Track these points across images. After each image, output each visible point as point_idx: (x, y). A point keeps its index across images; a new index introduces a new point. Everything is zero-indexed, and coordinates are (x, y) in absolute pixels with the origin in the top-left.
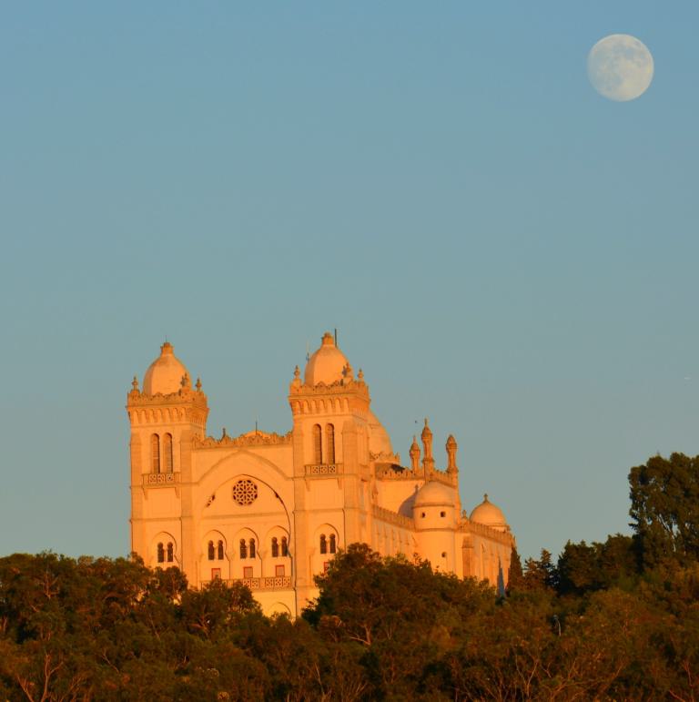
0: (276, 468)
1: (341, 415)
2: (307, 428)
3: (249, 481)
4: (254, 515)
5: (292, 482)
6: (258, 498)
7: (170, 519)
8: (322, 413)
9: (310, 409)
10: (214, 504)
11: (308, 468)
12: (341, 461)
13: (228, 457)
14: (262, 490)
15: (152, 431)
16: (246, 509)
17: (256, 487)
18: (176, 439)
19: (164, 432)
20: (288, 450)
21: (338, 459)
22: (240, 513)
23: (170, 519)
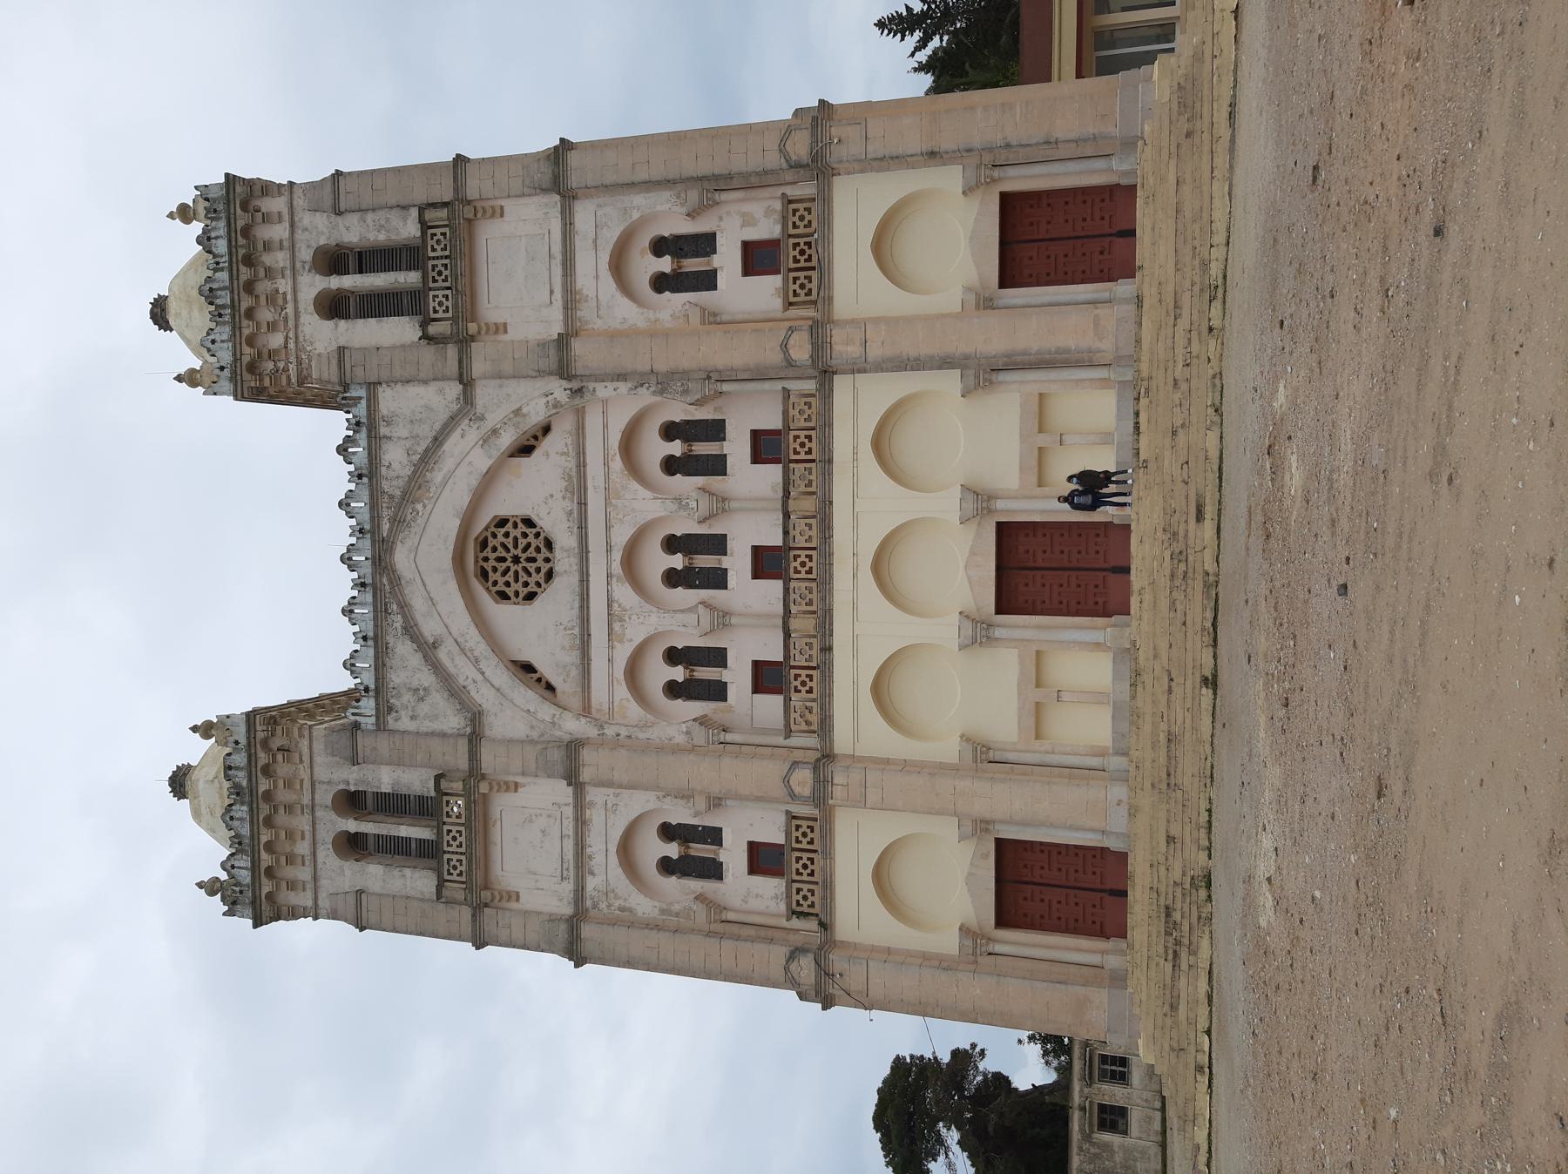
0: (438, 440)
1: (292, 225)
2: (322, 335)
3: (484, 544)
4: (582, 527)
5: (485, 394)
6: (535, 519)
7: (581, 823)
8: (284, 285)
9: (272, 327)
10: (546, 669)
11: (433, 329)
12: (414, 212)
13: (404, 607)
14: (508, 501)
15: (327, 857)
16: (564, 562)
17: (502, 522)
18: (352, 778)
19: (333, 816)
20: (389, 399)
21: (408, 229)
22: (575, 579)
23: (581, 823)
